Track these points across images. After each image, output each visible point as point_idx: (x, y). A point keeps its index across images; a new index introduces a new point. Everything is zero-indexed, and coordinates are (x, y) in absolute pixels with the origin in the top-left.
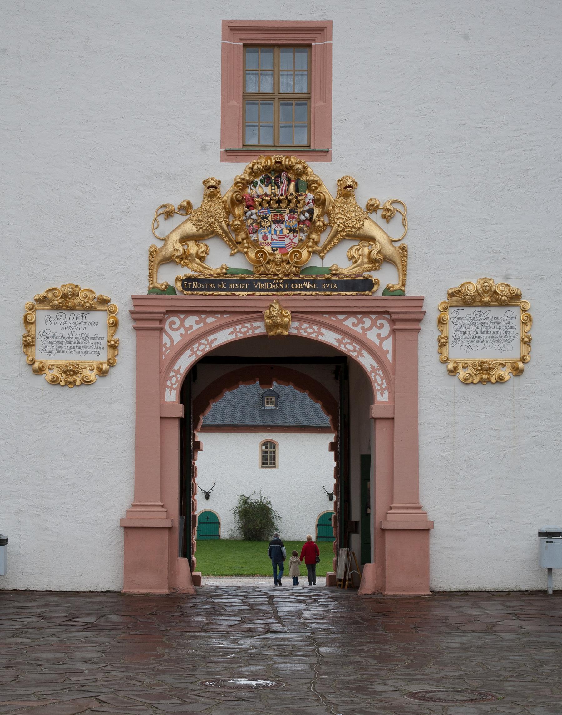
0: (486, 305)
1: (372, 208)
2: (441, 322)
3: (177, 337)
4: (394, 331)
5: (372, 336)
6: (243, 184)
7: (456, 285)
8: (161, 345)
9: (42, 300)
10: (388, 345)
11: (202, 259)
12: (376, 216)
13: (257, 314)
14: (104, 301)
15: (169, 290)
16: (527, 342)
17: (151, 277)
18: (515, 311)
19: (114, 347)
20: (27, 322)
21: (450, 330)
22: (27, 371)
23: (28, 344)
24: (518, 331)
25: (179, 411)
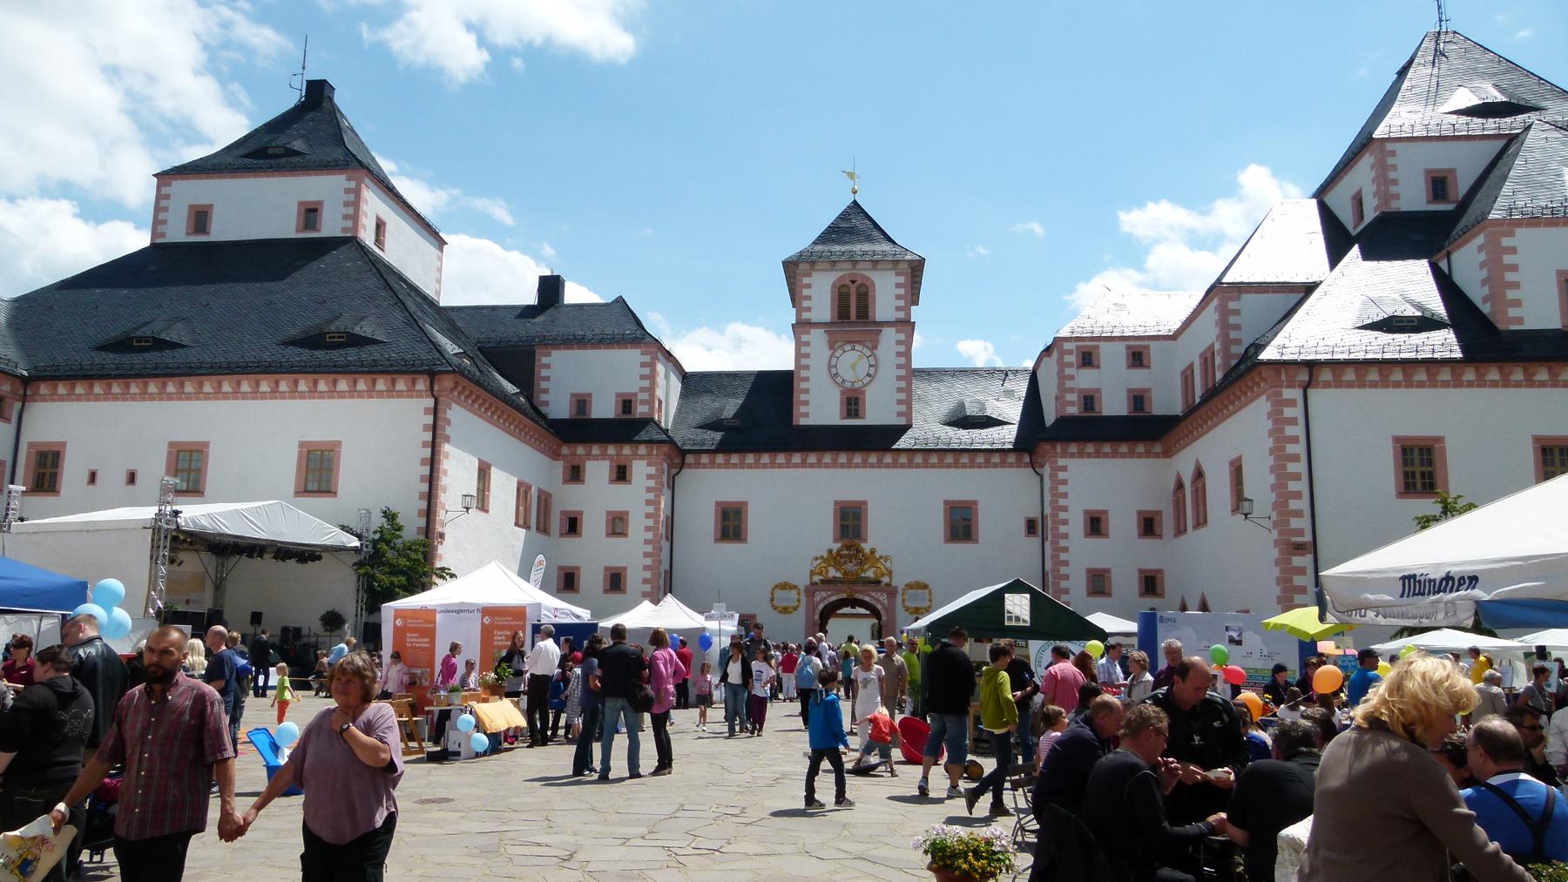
0: (917, 589)
1: (881, 557)
2: (903, 594)
3: (819, 599)
4: (888, 597)
5: (881, 598)
6: (839, 551)
7: (907, 582)
8: (813, 601)
9: (776, 586)
10: (886, 602)
11: (827, 573)
12: (882, 561)
13: (843, 592)
14: (796, 587)
15: (816, 584)
16: (930, 601)
17: (811, 579)
18: (927, 591)
19: (799, 601)
20: (772, 594)
21: (906, 597)
22: (772, 609)
23: (772, 600)
24: (928, 597)
25: (819, 622)
